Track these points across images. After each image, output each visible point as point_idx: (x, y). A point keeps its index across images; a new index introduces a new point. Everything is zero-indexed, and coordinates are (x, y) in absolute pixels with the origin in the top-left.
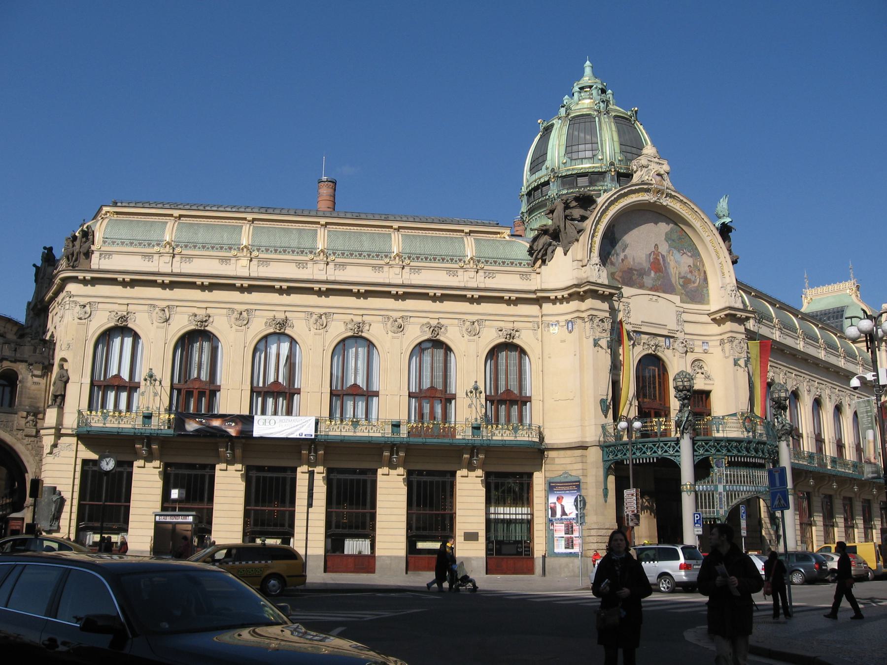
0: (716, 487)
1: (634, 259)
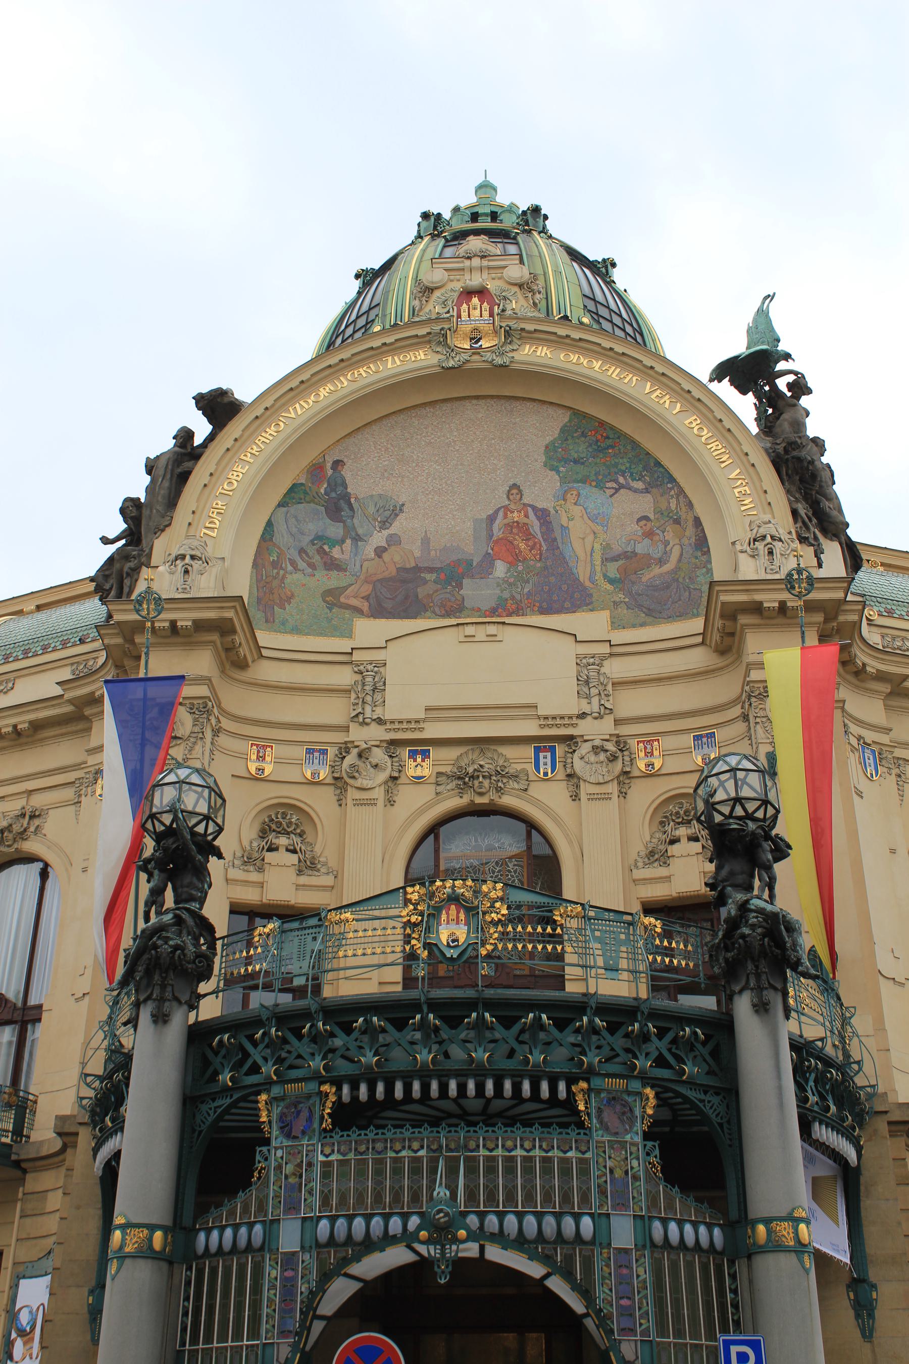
0: (271, 1225)
1: (426, 541)
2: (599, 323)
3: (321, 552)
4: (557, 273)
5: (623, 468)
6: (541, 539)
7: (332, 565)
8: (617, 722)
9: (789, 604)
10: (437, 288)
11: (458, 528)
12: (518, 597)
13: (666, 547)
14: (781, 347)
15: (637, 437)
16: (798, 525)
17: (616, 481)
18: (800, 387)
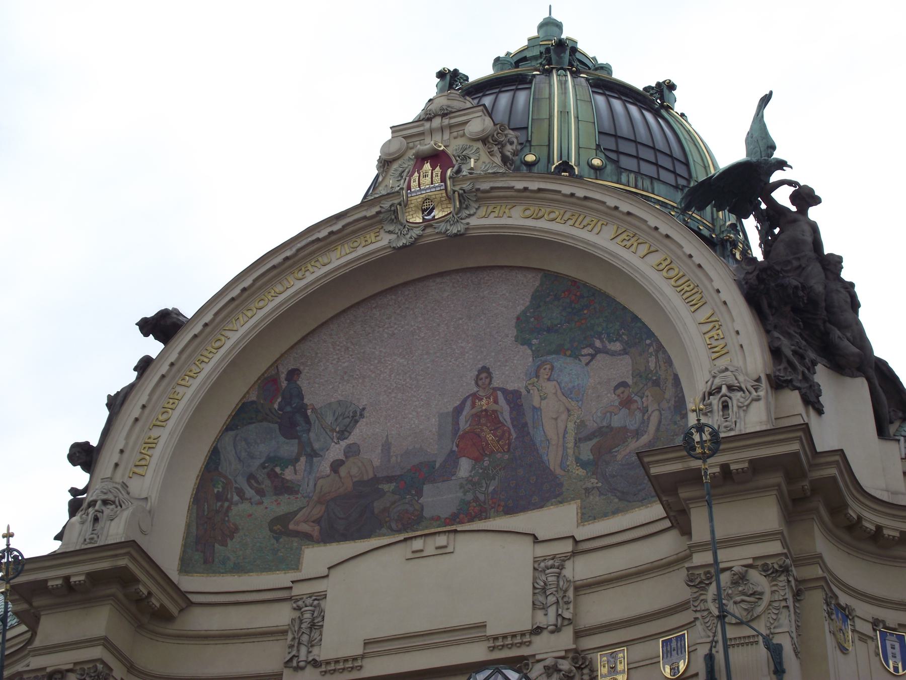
1: (387, 447)
2: (616, 162)
3: (273, 475)
4: (564, 113)
5: (600, 329)
6: (511, 427)
7: (284, 488)
8: (579, 634)
9: (733, 467)
10: (395, 160)
11: (421, 427)
12: (482, 497)
13: (643, 416)
14: (777, 155)
15: (611, 292)
16: (782, 367)
17: (592, 346)
18: (805, 197)
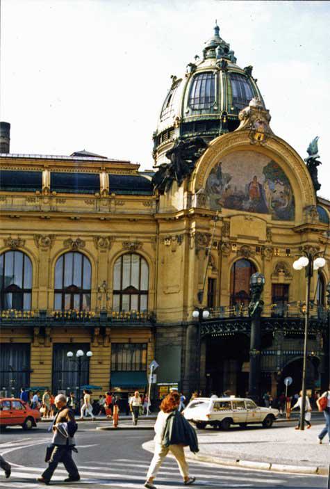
1: (236, 188)
7: (218, 192)
18: (318, 163)
